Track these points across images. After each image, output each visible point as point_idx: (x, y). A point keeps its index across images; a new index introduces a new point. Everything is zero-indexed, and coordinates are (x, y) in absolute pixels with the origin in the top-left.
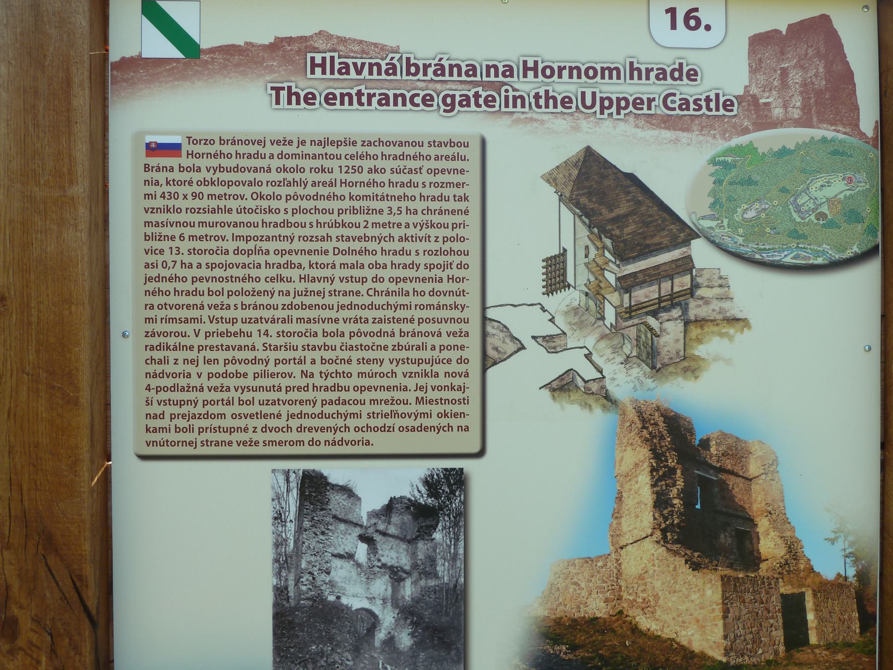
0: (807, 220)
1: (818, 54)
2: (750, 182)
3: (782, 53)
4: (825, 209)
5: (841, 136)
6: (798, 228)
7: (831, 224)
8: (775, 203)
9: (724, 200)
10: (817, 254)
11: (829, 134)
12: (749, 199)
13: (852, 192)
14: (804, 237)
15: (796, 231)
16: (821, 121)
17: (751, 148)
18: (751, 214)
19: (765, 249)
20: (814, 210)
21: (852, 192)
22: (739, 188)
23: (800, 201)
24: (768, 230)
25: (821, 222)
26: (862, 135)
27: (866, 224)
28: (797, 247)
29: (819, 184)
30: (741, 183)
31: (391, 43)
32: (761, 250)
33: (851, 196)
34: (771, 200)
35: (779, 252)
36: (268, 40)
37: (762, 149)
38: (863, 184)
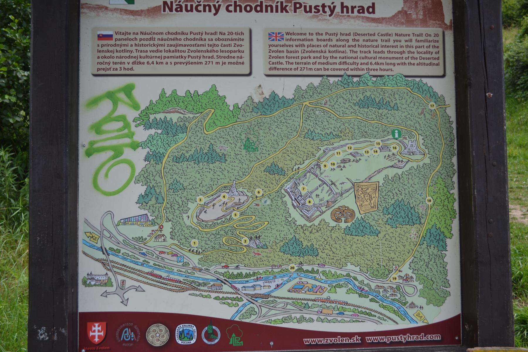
0: (316, 222)
2: (212, 156)
4: (349, 201)
6: (301, 236)
7: (362, 228)
8: (259, 191)
9: (164, 190)
12: (211, 187)
13: (400, 172)
14: (312, 251)
15: (296, 241)
18: (213, 214)
19: (240, 275)
20: (328, 205)
21: (400, 172)
23: (304, 189)
25: (343, 225)
27: (426, 227)
28: (300, 270)
29: (337, 159)
30: (196, 159)
32: (232, 276)
33: (399, 177)
34: (251, 186)
35: (267, 280)
38: (419, 157)
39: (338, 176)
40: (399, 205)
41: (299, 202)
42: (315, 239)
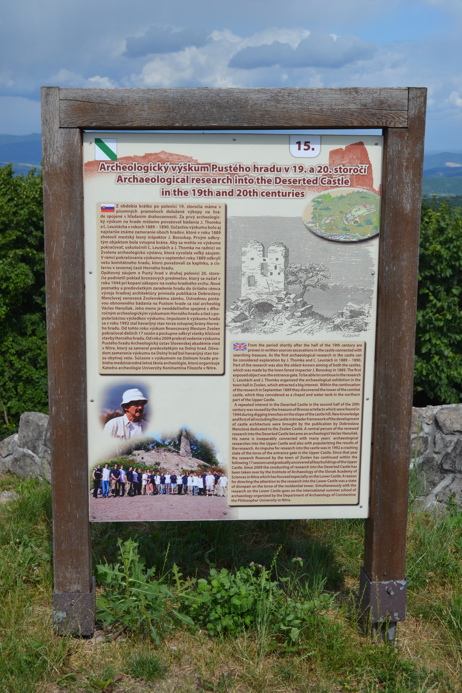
1: (357, 158)
2: (328, 209)
3: (343, 157)
4: (357, 219)
5: (365, 191)
7: (360, 225)
8: (338, 217)
10: (354, 237)
11: (361, 190)
16: (357, 185)
17: (329, 196)
18: (328, 221)
22: (323, 212)
23: (348, 216)
24: (334, 227)
26: (374, 190)
29: (355, 210)
30: (324, 209)
31: (189, 155)
36: (142, 154)
37: (333, 196)
40: (368, 220)
41: (347, 220)
42: (349, 228)
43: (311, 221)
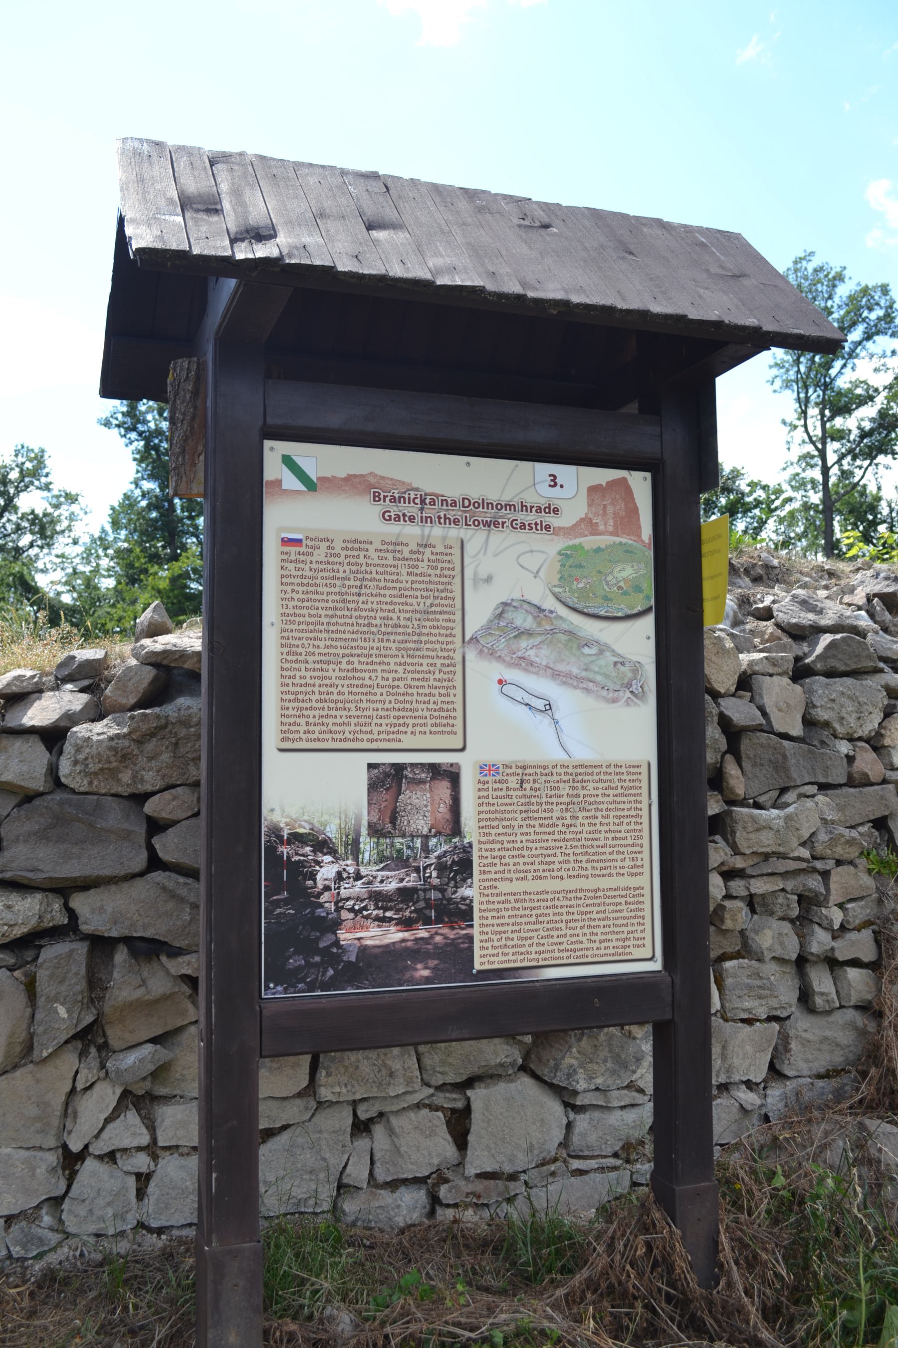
2: (580, 566)
4: (622, 584)
7: (625, 593)
11: (624, 540)
14: (611, 600)
22: (574, 570)
23: (609, 579)
39: (619, 575)
43: (558, 583)
